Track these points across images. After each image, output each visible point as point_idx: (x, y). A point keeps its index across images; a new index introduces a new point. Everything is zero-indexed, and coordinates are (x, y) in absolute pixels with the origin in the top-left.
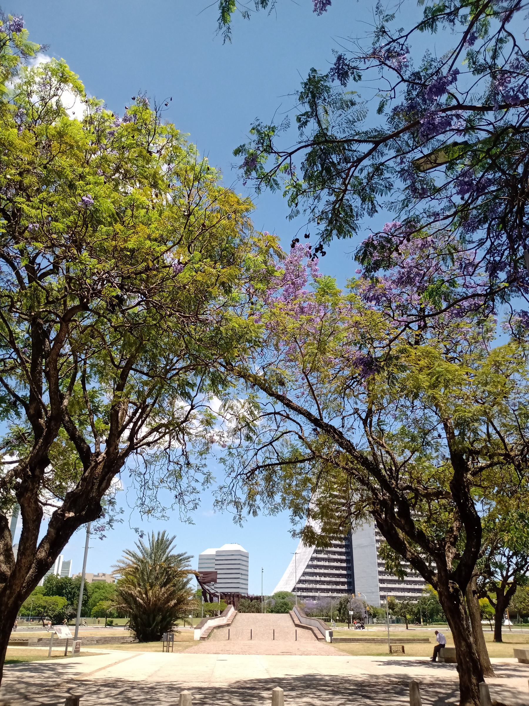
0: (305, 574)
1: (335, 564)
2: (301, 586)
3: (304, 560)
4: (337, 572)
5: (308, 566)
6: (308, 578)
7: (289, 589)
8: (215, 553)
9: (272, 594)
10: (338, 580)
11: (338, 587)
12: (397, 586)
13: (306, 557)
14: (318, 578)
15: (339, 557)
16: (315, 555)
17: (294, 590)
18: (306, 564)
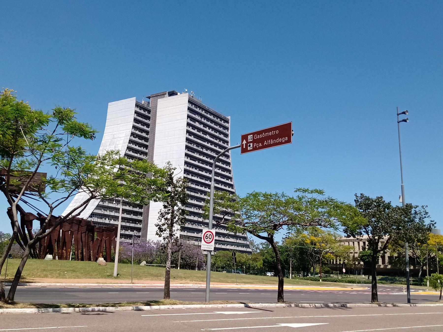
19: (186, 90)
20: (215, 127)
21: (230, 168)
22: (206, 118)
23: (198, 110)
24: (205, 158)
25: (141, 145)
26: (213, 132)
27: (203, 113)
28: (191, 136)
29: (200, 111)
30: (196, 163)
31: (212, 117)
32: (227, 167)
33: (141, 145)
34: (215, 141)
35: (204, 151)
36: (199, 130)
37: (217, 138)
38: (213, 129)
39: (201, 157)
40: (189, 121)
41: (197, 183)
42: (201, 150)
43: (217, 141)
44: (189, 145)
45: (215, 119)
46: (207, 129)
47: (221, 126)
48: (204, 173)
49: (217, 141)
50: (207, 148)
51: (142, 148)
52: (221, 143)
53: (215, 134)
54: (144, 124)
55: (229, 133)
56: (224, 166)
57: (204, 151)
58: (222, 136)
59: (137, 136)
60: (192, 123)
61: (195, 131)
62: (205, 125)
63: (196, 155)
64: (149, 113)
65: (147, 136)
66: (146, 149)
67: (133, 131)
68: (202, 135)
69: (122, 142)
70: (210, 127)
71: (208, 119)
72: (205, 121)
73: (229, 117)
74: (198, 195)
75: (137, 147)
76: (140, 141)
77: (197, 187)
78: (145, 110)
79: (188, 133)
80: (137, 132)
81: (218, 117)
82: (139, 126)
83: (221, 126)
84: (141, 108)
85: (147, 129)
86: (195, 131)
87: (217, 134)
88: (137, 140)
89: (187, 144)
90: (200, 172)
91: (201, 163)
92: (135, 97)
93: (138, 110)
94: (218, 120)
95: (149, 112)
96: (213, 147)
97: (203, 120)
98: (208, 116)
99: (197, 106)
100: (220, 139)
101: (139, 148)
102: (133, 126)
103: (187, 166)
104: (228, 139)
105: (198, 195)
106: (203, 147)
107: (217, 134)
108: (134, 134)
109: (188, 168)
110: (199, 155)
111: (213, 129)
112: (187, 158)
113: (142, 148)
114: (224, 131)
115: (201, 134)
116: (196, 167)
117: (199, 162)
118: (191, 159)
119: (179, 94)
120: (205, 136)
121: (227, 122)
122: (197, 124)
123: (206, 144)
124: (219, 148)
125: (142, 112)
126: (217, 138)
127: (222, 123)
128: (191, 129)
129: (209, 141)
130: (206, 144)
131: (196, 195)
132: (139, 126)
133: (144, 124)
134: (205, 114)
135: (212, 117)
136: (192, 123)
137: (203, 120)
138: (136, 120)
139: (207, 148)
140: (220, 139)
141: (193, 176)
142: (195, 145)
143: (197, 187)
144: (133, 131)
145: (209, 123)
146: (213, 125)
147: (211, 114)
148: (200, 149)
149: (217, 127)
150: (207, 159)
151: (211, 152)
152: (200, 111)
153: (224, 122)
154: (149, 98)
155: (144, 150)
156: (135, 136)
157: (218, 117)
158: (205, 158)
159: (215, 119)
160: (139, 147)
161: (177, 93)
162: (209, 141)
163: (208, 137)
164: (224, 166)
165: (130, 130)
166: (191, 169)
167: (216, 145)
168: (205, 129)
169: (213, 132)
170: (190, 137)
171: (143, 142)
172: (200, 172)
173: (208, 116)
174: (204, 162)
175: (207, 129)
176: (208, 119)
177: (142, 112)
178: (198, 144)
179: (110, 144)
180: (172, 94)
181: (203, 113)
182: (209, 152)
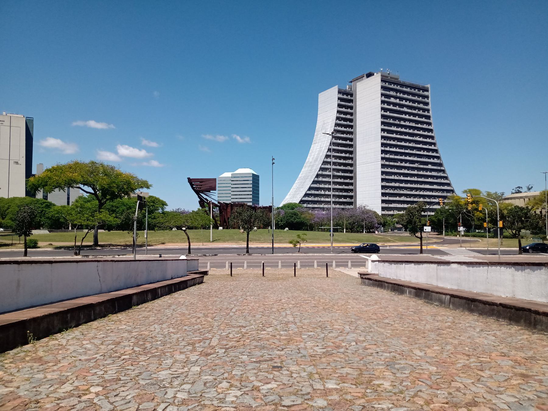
0: (310, 189)
1: (339, 180)
2: (306, 199)
3: (309, 177)
4: (341, 187)
5: (314, 182)
6: (313, 192)
7: (297, 202)
8: (231, 176)
9: (281, 206)
10: (341, 194)
11: (341, 200)
12: (397, 198)
13: (312, 174)
14: (323, 192)
15: (343, 174)
16: (320, 173)
17: (300, 202)
18: (312, 180)
19: (382, 69)
20: (413, 98)
21: (433, 135)
22: (401, 92)
23: (392, 86)
24: (403, 130)
25: (346, 126)
26: (411, 104)
27: (399, 88)
28: (386, 112)
29: (395, 87)
30: (394, 136)
31: (408, 90)
32: (430, 134)
33: (346, 126)
34: (414, 112)
36: (395, 104)
37: (415, 108)
38: (410, 100)
39: (399, 129)
40: (383, 98)
41: (396, 153)
42: (399, 123)
43: (416, 112)
44: (385, 121)
45: (413, 91)
46: (404, 102)
47: (419, 96)
48: (403, 144)
49: (416, 112)
50: (405, 120)
51: (348, 128)
52: (421, 112)
53: (413, 105)
54: (347, 107)
56: (426, 133)
57: (402, 123)
58: (421, 106)
59: (342, 119)
60: (386, 100)
61: (391, 107)
62: (401, 99)
63: (394, 129)
64: (352, 97)
65: (351, 117)
66: (352, 129)
67: (338, 115)
68: (399, 109)
69: (329, 126)
70: (407, 100)
71: (404, 93)
72: (401, 95)
73: (429, 86)
74: (399, 164)
75: (343, 129)
76: (345, 123)
77: (396, 157)
78: (347, 94)
79: (383, 110)
80: (342, 116)
81: (415, 88)
82: (344, 110)
83: (419, 96)
85: (351, 111)
86: (391, 107)
87: (416, 105)
88: (342, 122)
89: (383, 120)
90: (399, 143)
91: (399, 135)
92: (337, 86)
93: (341, 96)
96: (412, 118)
97: (398, 94)
98: (404, 89)
99: (390, 83)
100: (420, 109)
101: (345, 129)
102: (337, 111)
103: (385, 140)
104: (429, 107)
105: (399, 164)
106: (400, 119)
107: (416, 105)
108: (339, 118)
109: (385, 142)
110: (397, 128)
111: (410, 100)
112: (384, 133)
113: (348, 128)
114: (423, 100)
115: (397, 108)
116: (394, 139)
117: (397, 134)
118: (388, 133)
119: (375, 74)
120: (401, 109)
121: (427, 90)
122: (392, 100)
123: (403, 116)
124: (419, 117)
125: (345, 97)
126: (415, 108)
127: (421, 92)
128: (386, 106)
129: (406, 113)
130: (403, 116)
131: (396, 164)
132: (344, 110)
133: (347, 107)
134: (401, 89)
135: (408, 90)
136: (386, 100)
137: (398, 94)
138: (339, 106)
139: (405, 120)
140: (420, 109)
141: (391, 148)
142: (392, 120)
143: (396, 157)
144: (338, 115)
145: (406, 96)
146: (410, 97)
147: (407, 86)
148: (397, 122)
149: (416, 98)
150: (405, 130)
151: (410, 123)
152: (395, 87)
153: (423, 92)
155: (350, 130)
156: (340, 119)
157: (415, 88)
158: (403, 130)
159: (413, 91)
160: (344, 128)
161: (374, 74)
162: (406, 113)
163: (405, 109)
164: (426, 133)
165: (334, 114)
166: (388, 142)
167: (415, 115)
168: (401, 102)
169: (411, 104)
170: (385, 113)
171: (348, 123)
172: (399, 143)
173: (404, 89)
174: (401, 133)
175: (404, 102)
176: (404, 93)
177: (345, 97)
178: (395, 118)
179: (321, 130)
180: (369, 75)
181: (399, 88)
182: (407, 123)
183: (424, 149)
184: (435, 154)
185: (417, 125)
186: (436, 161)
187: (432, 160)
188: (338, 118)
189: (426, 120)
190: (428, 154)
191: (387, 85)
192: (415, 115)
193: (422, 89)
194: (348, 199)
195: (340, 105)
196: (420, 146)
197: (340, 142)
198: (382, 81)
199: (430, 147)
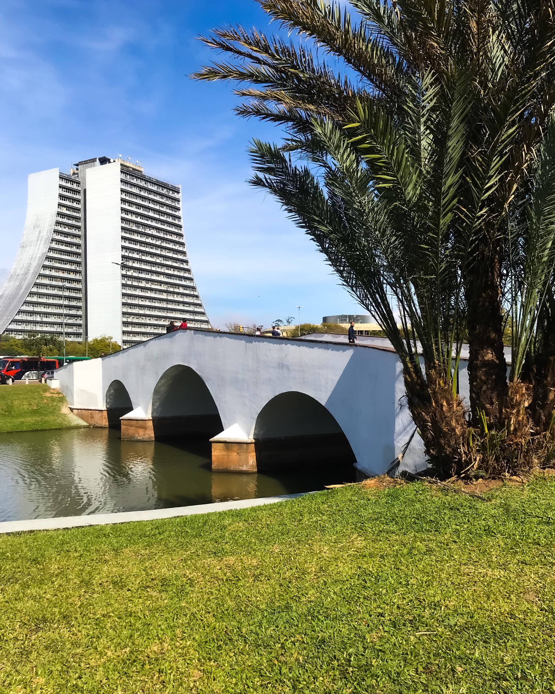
19: (120, 156)
21: (184, 250)
31: (155, 188)
32: (181, 249)
35: (146, 232)
39: (144, 239)
42: (143, 231)
45: (160, 190)
55: (180, 205)
56: (177, 247)
61: (133, 209)
63: (138, 238)
73: (180, 187)
75: (66, 230)
78: (73, 182)
84: (68, 180)
86: (133, 209)
88: (65, 220)
93: (64, 183)
94: (165, 191)
95: (78, 183)
119: (112, 161)
121: (178, 193)
125: (69, 185)
127: (171, 194)
128: (127, 207)
135: (155, 188)
140: (169, 215)
149: (164, 200)
154: (77, 165)
158: (149, 240)
163: (151, 214)
164: (177, 247)
167: (163, 222)
170: (126, 216)
176: (150, 191)
177: (69, 185)
180: (104, 161)
183: (175, 268)
184: (187, 275)
185: (165, 236)
186: (188, 283)
187: (183, 283)
188: (59, 214)
189: (176, 231)
190: (178, 274)
191: (128, 178)
192: (163, 222)
193: (171, 190)
194: (75, 328)
195: (63, 197)
196: (169, 263)
197: (63, 248)
198: (121, 172)
199: (182, 266)
